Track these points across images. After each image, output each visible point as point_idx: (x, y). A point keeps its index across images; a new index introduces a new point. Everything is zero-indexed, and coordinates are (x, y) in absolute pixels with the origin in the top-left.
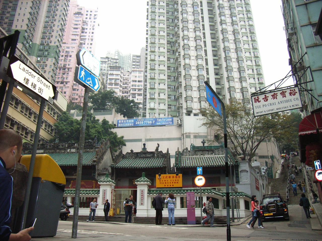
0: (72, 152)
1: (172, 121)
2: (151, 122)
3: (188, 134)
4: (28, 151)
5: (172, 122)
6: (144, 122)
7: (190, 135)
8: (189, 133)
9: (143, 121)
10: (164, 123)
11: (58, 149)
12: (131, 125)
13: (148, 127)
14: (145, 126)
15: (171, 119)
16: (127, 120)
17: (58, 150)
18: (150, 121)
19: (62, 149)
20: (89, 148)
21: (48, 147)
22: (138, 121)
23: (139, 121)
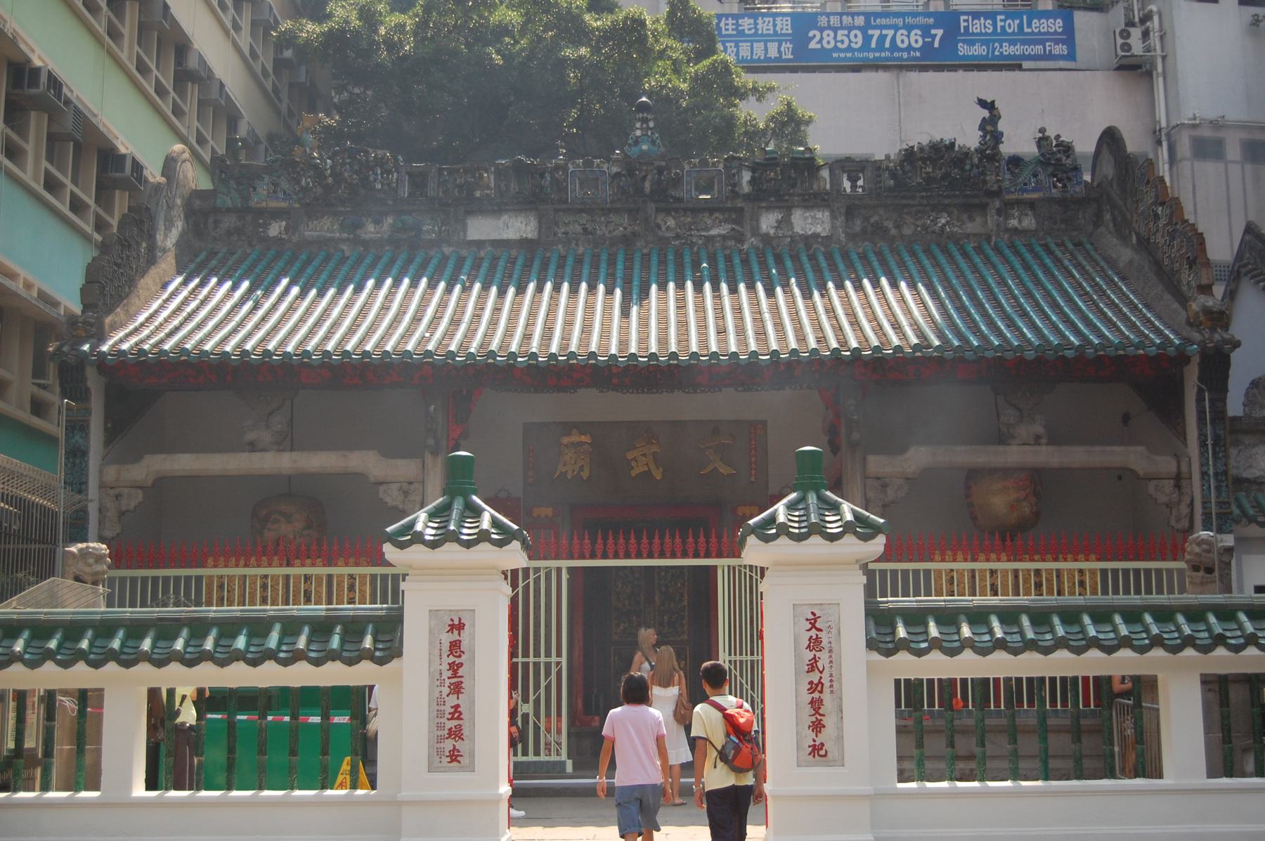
0: (809, 240)
1: (1068, 35)
2: (916, 39)
3: (1206, 133)
4: (390, 220)
5: (1063, 42)
6: (867, 39)
7: (1220, 135)
8: (1216, 124)
9: (864, 30)
10: (1008, 49)
11: (668, 212)
12: (773, 53)
13: (914, 76)
14: (886, 68)
15: (1059, 22)
16: (742, 16)
17: (671, 222)
18: (909, 28)
19: (709, 208)
20: (945, 208)
21: (575, 191)
22: (821, 30)
23: (835, 30)
